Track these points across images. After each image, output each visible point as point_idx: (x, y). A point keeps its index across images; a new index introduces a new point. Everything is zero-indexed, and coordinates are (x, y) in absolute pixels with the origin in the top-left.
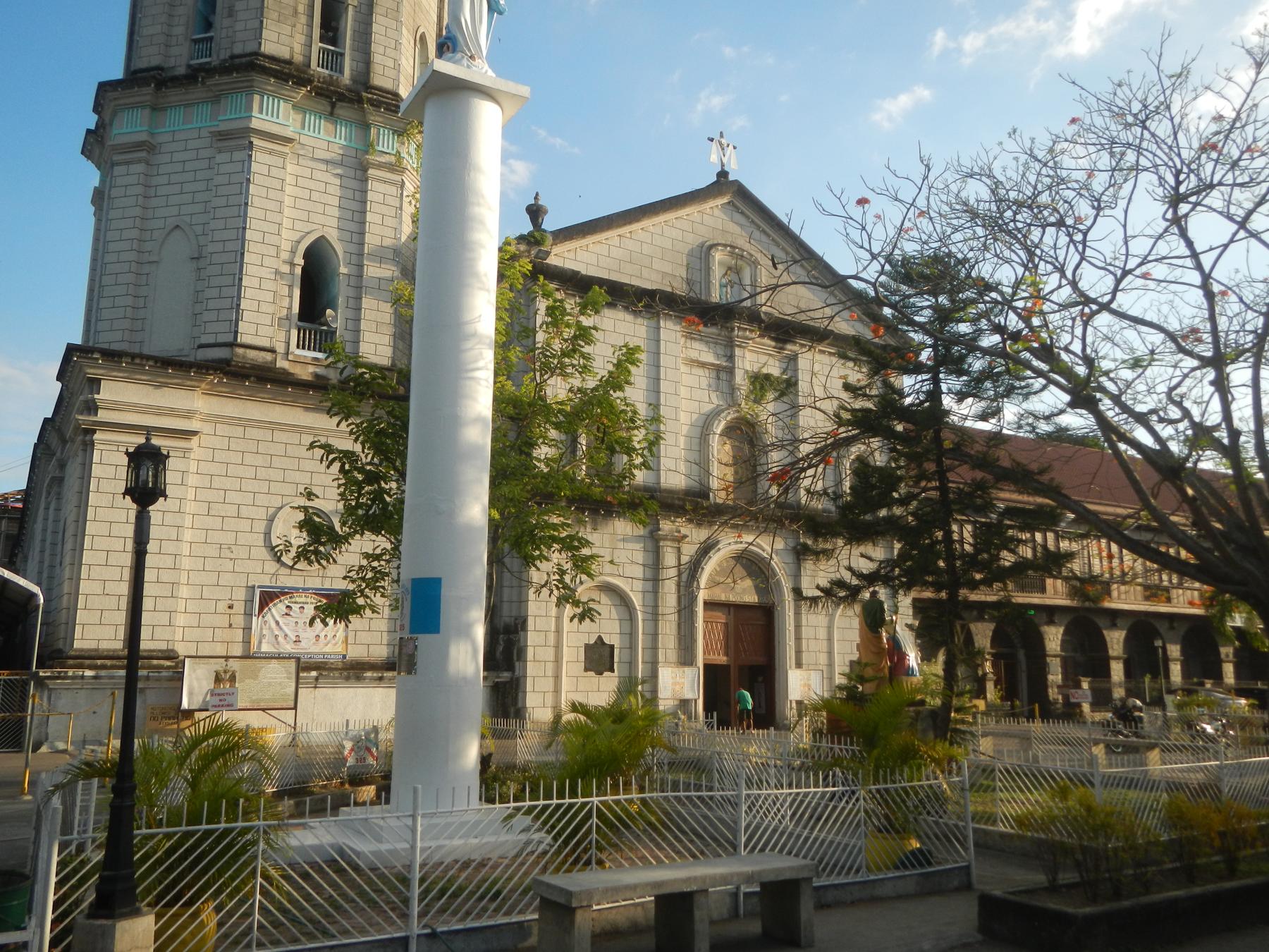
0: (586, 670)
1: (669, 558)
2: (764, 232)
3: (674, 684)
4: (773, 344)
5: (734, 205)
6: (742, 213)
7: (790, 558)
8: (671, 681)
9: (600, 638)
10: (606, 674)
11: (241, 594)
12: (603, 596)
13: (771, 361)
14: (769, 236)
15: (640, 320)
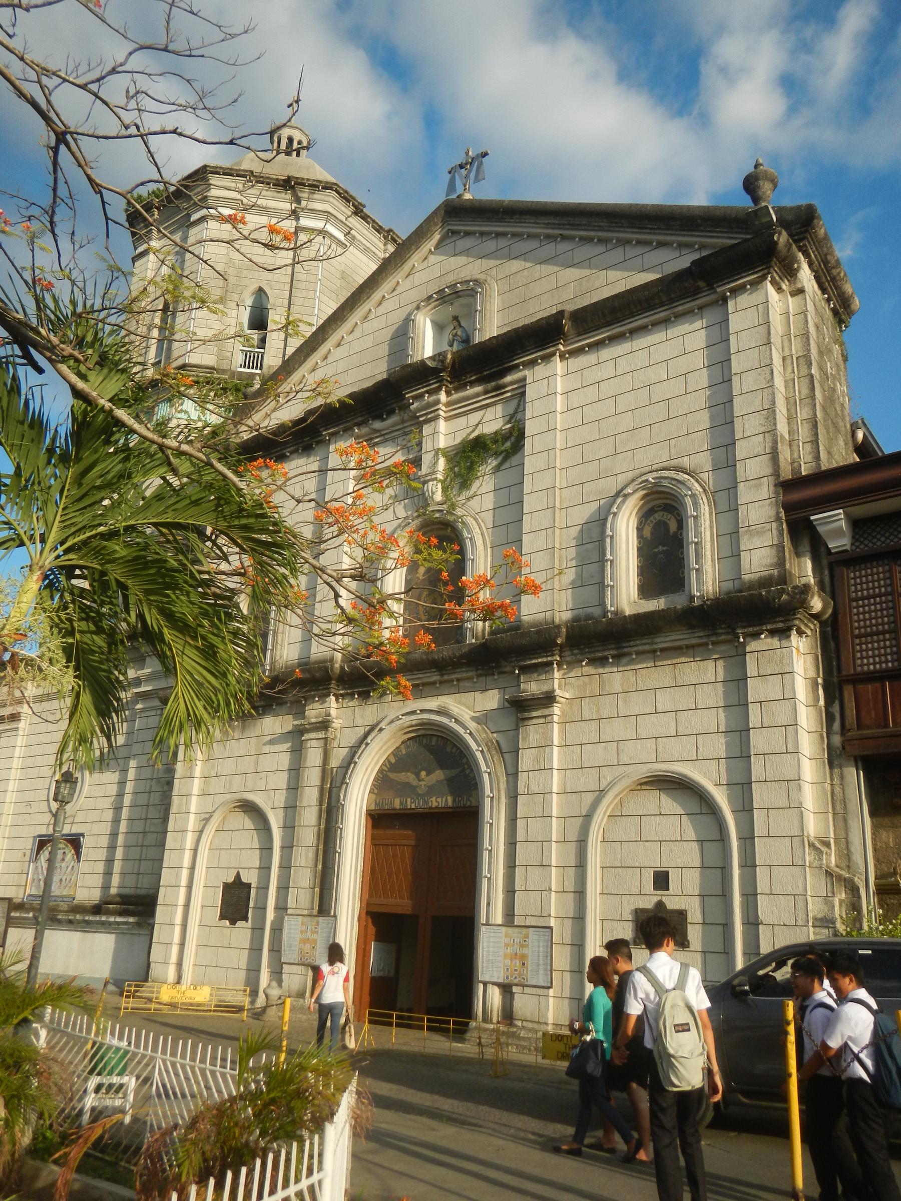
0: (222, 917)
1: (314, 756)
2: (498, 235)
3: (304, 941)
4: (478, 389)
5: (454, 232)
6: (468, 234)
7: (506, 723)
8: (299, 936)
9: (238, 875)
10: (240, 924)
11: (29, 844)
12: (246, 818)
13: (490, 413)
14: (504, 234)
15: (312, 459)
